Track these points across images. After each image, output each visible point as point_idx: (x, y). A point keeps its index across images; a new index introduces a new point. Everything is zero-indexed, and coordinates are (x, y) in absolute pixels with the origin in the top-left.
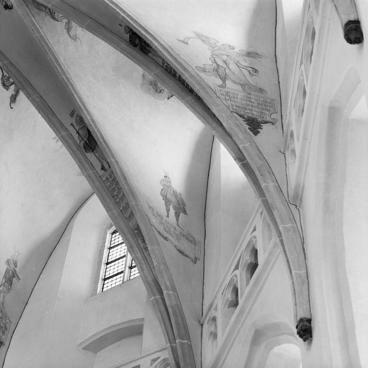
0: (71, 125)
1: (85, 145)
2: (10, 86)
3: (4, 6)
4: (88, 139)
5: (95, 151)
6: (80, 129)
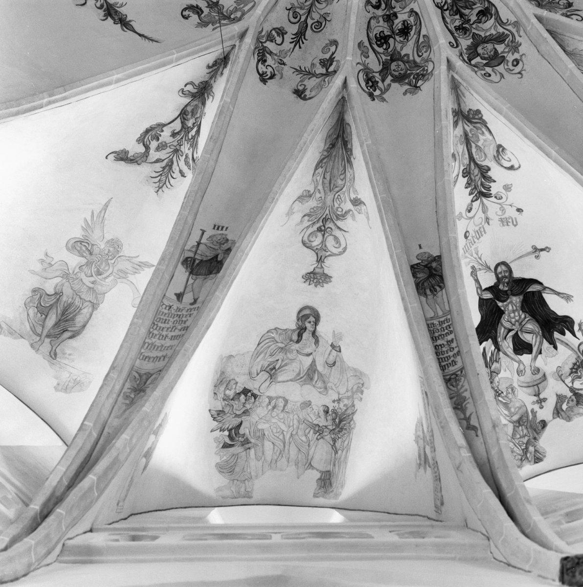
1: (189, 259)
2: (144, 145)
3: (296, 89)
4: (202, 260)
5: (194, 277)
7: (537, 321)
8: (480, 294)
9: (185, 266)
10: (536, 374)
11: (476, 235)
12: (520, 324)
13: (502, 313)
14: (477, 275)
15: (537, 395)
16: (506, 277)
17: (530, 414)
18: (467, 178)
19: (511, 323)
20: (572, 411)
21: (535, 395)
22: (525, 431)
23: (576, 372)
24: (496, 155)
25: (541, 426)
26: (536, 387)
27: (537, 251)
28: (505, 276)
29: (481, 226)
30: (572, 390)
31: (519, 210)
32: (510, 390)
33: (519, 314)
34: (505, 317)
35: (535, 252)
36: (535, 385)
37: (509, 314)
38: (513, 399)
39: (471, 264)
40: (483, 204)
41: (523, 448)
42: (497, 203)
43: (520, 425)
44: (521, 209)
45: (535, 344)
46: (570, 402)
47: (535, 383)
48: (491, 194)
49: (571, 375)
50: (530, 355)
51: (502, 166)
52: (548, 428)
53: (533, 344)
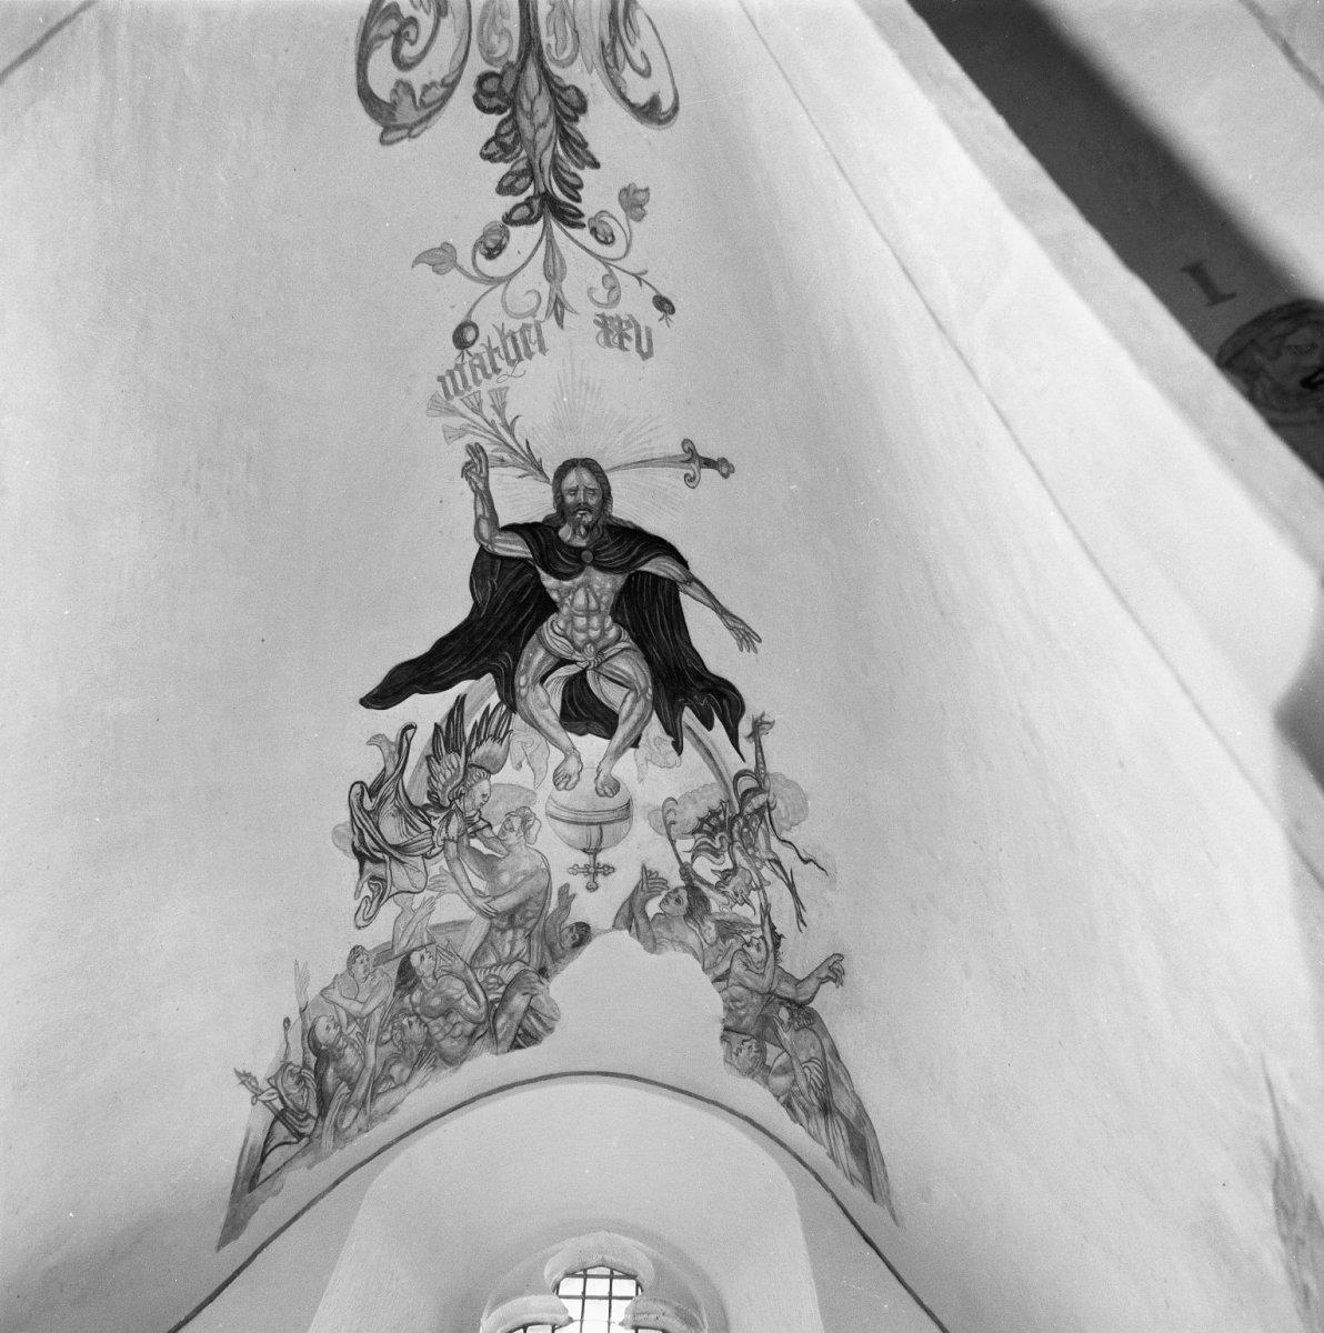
7: (649, 659)
8: (486, 536)
10: (606, 794)
11: (505, 347)
12: (600, 652)
13: (549, 607)
14: (487, 478)
15: (593, 851)
16: (589, 509)
17: (555, 897)
18: (496, 119)
19: (572, 642)
20: (669, 929)
21: (584, 851)
22: (521, 945)
23: (711, 836)
24: (607, 40)
25: (574, 938)
26: (595, 829)
27: (694, 460)
28: (586, 503)
29: (529, 320)
30: (686, 872)
31: (663, 304)
32: (516, 822)
33: (602, 623)
34: (557, 622)
35: (688, 461)
36: (592, 824)
37: (571, 621)
38: (517, 849)
39: (470, 439)
40: (551, 242)
41: (491, 997)
42: (598, 257)
43: (512, 926)
44: (670, 303)
45: (627, 719)
46: (672, 902)
47: (598, 818)
48: (581, 215)
49: (698, 836)
50: (607, 742)
51: (624, 98)
52: (588, 951)
53: (623, 714)
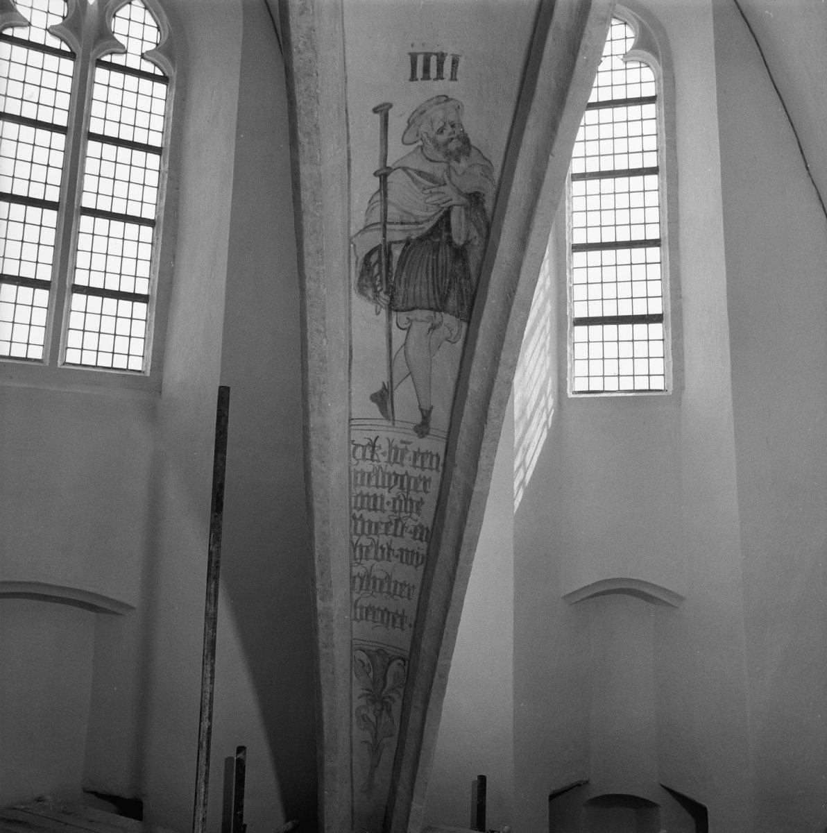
0: (375, 111)
1: (374, 258)
4: (408, 242)
6: (405, 169)
9: (370, 293)
